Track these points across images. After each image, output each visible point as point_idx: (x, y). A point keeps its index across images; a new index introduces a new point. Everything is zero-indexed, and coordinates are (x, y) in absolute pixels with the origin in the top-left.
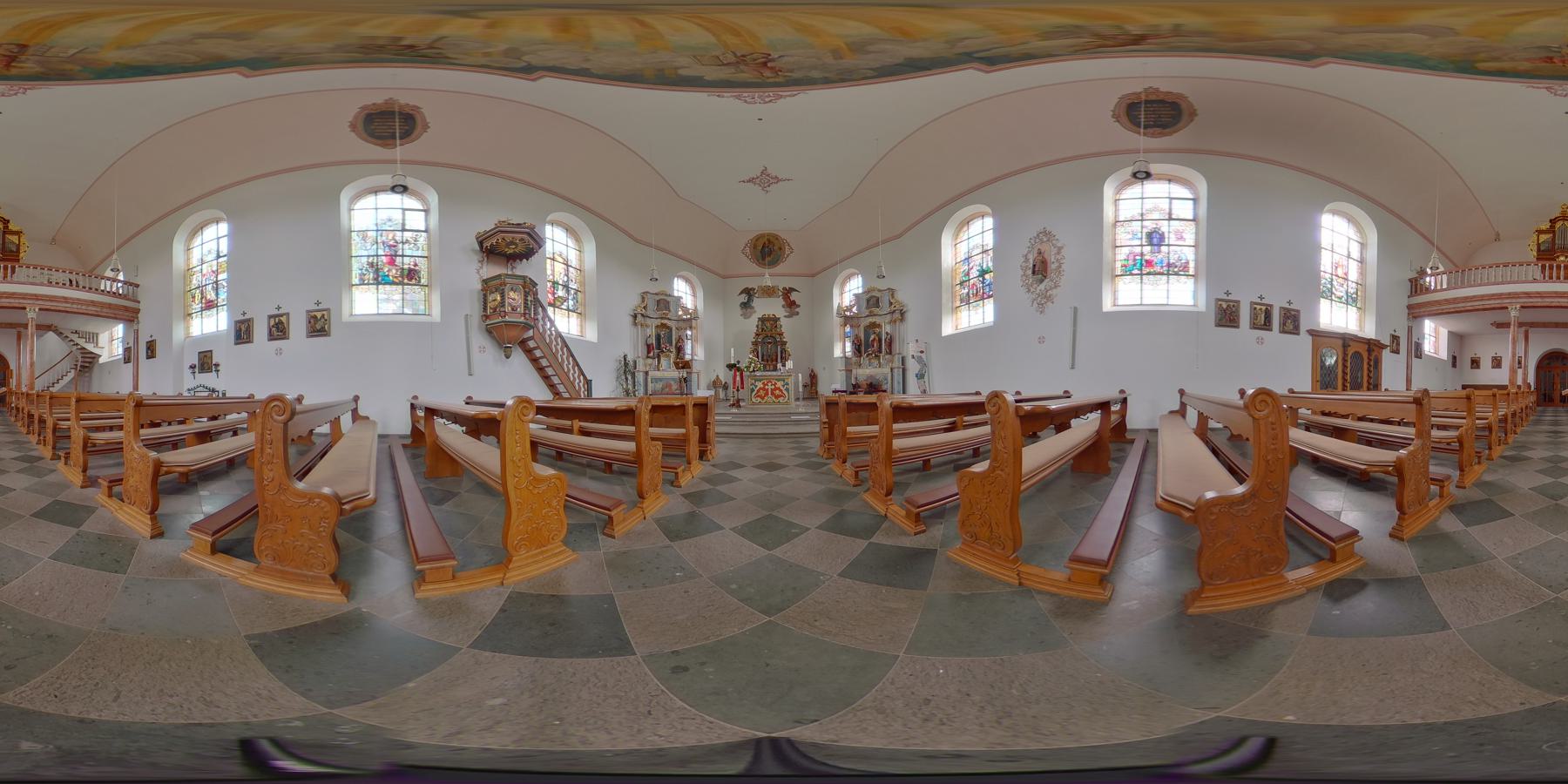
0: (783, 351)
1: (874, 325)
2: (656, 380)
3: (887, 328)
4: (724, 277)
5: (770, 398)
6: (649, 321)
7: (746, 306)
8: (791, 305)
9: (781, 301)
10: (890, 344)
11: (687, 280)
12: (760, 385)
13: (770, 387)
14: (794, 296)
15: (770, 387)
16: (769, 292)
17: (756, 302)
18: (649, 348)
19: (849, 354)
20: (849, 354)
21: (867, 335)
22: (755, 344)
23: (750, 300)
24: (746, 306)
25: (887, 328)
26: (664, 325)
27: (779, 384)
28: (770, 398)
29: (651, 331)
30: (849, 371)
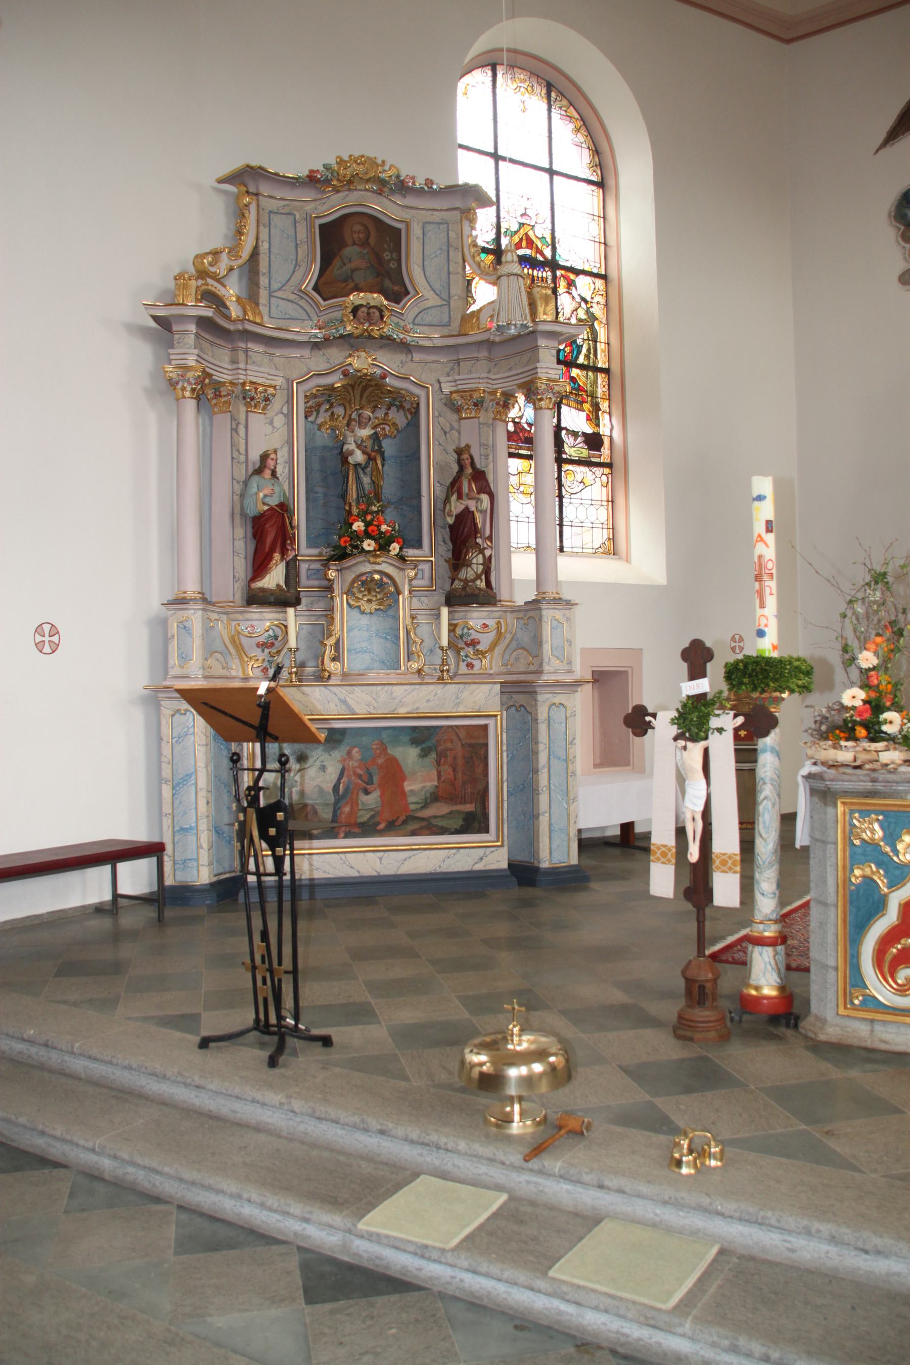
6: (261, 369)
11: (556, 86)
18: (268, 533)
26: (365, 390)
29: (279, 434)
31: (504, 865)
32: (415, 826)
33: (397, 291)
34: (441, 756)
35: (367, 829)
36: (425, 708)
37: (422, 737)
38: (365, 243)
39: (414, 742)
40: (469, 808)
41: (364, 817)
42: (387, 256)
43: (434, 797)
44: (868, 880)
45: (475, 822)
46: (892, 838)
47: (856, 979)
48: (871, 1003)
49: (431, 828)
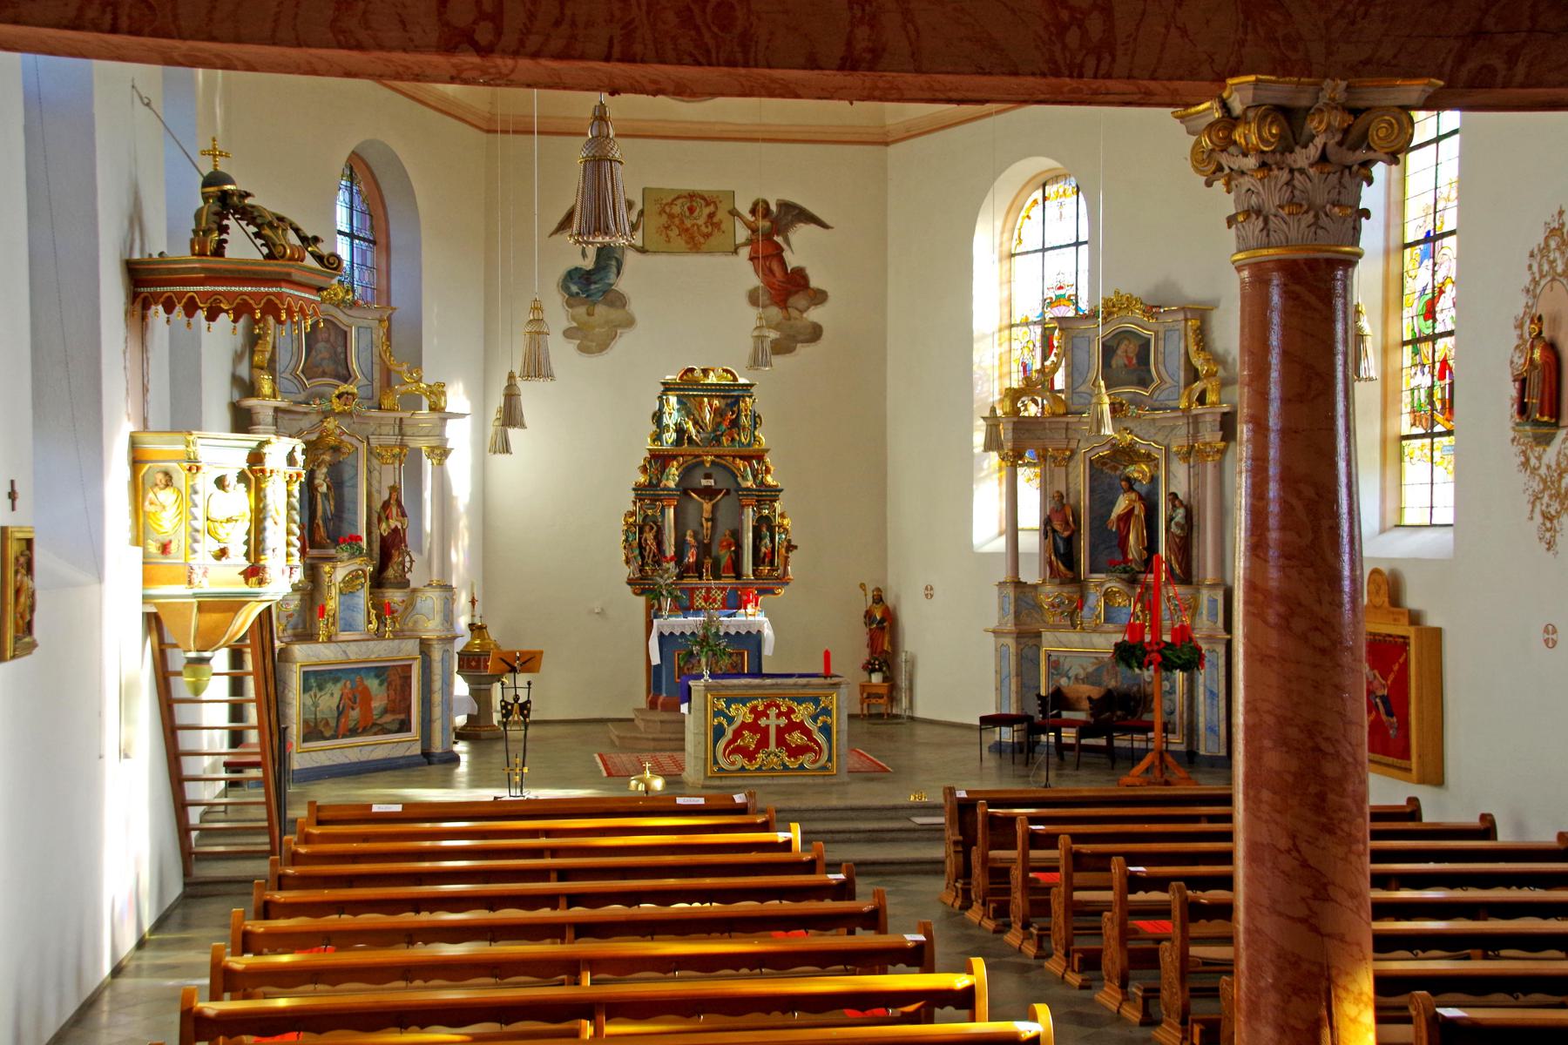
0: (765, 525)
1: (1127, 454)
2: (315, 679)
3: (1179, 479)
4: (488, 131)
5: (773, 755)
7: (590, 285)
8: (787, 288)
9: (742, 273)
10: (1185, 546)
12: (742, 714)
13: (772, 722)
14: (800, 248)
15: (772, 722)
16: (690, 222)
17: (636, 277)
19: (1031, 574)
20: (1031, 574)
21: (1102, 496)
22: (647, 493)
23: (608, 259)
24: (590, 285)
25: (1179, 479)
27: (802, 713)
28: (773, 755)
30: (1027, 638)
31: (419, 752)
32: (375, 729)
33: (346, 377)
34: (390, 684)
35: (353, 732)
36: (384, 655)
37: (380, 672)
38: (328, 341)
39: (377, 676)
40: (402, 716)
41: (352, 724)
42: (340, 349)
43: (385, 711)
44: (720, 724)
45: (404, 726)
46: (728, 707)
47: (716, 762)
48: (721, 769)
49: (385, 731)
